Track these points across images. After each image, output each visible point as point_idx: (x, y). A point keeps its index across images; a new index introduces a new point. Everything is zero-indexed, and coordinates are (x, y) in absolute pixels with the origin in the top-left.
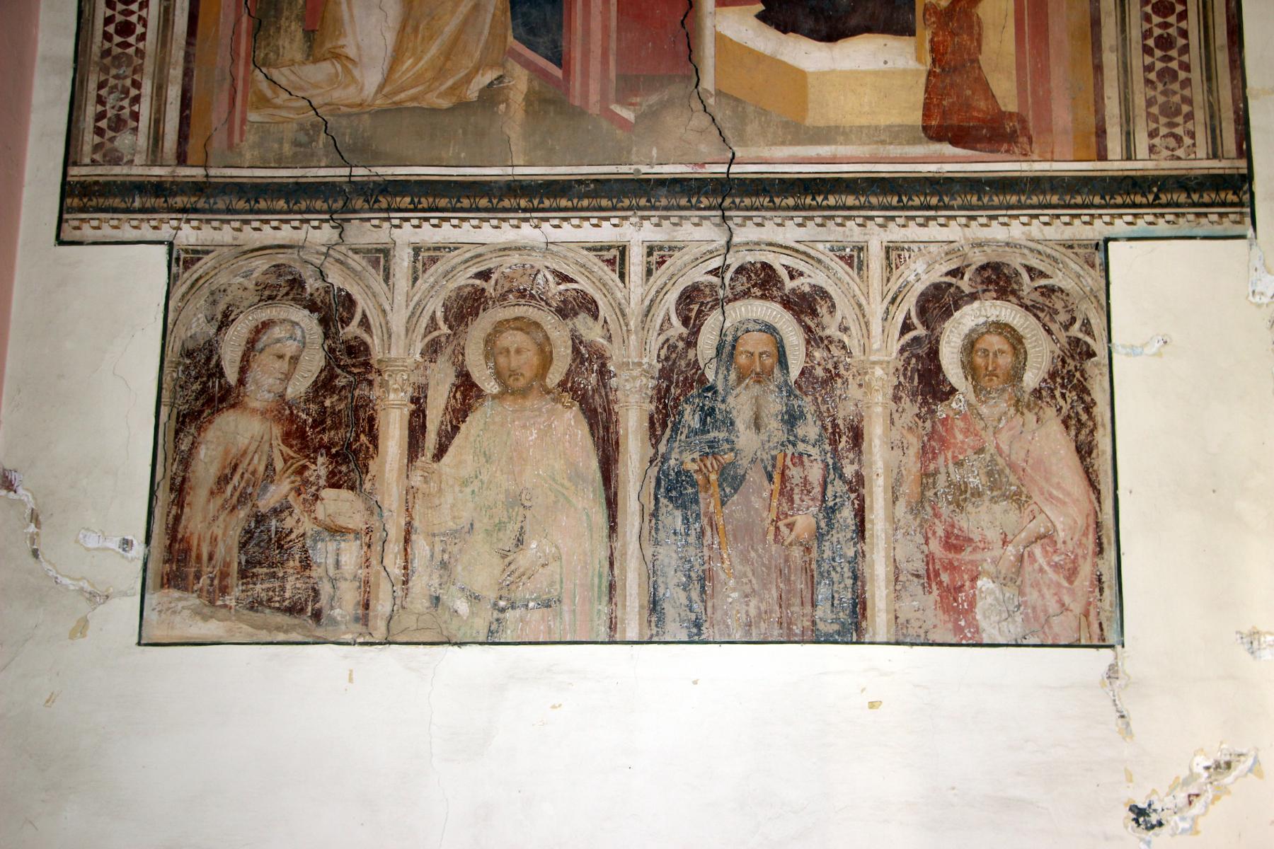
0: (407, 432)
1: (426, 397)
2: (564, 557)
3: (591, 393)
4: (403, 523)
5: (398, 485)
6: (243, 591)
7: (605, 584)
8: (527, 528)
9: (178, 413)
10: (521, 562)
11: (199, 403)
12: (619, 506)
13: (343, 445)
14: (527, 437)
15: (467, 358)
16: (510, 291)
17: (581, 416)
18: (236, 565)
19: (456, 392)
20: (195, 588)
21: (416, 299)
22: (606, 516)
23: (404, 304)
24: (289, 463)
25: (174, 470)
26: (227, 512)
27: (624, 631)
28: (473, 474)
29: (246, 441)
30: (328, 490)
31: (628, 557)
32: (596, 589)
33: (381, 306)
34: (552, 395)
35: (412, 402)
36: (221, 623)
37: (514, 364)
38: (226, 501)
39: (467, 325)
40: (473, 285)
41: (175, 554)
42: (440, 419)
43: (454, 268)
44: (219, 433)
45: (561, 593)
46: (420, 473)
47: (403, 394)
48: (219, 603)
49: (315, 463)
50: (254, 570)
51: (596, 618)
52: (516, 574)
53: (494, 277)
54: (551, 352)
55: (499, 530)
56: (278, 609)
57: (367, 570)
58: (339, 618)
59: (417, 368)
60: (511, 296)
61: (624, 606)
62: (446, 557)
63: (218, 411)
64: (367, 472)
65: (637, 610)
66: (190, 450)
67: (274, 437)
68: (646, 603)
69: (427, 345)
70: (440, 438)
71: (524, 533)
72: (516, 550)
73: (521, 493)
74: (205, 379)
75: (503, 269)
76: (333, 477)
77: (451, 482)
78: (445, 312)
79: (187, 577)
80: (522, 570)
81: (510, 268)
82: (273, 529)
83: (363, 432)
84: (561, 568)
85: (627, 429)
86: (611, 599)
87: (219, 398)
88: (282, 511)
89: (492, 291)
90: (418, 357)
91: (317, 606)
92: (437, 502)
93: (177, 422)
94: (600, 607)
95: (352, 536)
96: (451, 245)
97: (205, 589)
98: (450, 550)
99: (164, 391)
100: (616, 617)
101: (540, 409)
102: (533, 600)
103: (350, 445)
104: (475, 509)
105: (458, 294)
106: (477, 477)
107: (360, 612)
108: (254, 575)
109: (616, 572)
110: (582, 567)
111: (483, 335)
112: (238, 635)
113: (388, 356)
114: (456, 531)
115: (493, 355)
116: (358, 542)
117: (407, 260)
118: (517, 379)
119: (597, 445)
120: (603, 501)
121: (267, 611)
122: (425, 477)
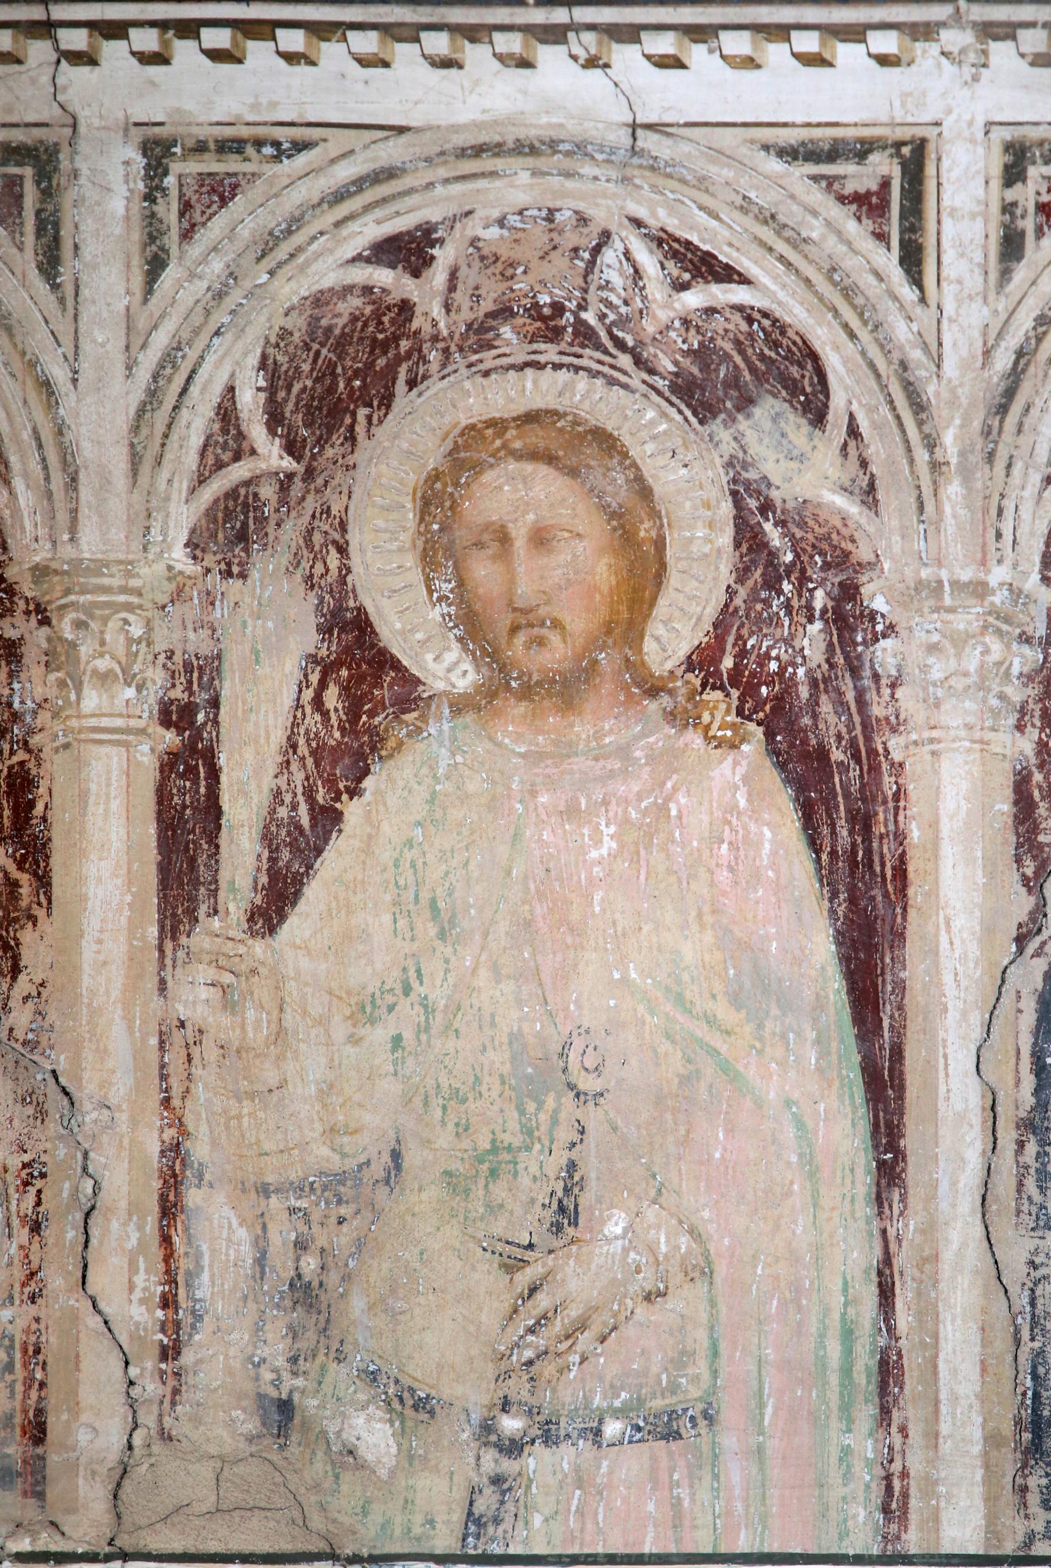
0: (152, 830)
1: (215, 703)
2: (721, 1270)
3: (804, 692)
4: (154, 1148)
7: (865, 1361)
8: (591, 1168)
10: (573, 1285)
12: (912, 1092)
14: (583, 851)
15: (356, 561)
16: (504, 312)
17: (772, 778)
19: (323, 685)
21: (161, 340)
22: (864, 1127)
23: (119, 360)
27: (935, 1518)
28: (393, 980)
31: (946, 1268)
32: (834, 1379)
33: (32, 364)
34: (665, 700)
35: (166, 721)
37: (525, 590)
39: (351, 438)
40: (368, 290)
42: (268, 782)
43: (294, 223)
45: (714, 1390)
46: (204, 973)
47: (130, 693)
51: (835, 1476)
52: (557, 1326)
53: (444, 256)
54: (660, 544)
55: (493, 1173)
59: (178, 595)
60: (506, 332)
61: (933, 1437)
62: (310, 1264)
65: (977, 1449)
68: (1007, 1428)
69: (210, 513)
70: (274, 852)
71: (581, 1184)
72: (557, 1243)
73: (567, 1045)
75: (474, 228)
77: (316, 1009)
78: (271, 390)
80: (574, 1312)
81: (501, 222)
84: (713, 1304)
85: (934, 825)
86: (885, 1412)
89: (437, 310)
90: (179, 556)
92: (272, 1077)
94: (848, 1440)
96: (280, 133)
98: (322, 1241)
100: (904, 1475)
101: (624, 752)
102: (618, 1413)
104: (407, 1101)
105: (314, 322)
106: (407, 990)
109: (903, 1320)
110: (783, 1304)
111: (413, 478)
113: (67, 551)
114: (341, 1178)
115: (449, 551)
117: (122, 190)
118: (541, 642)
119: (827, 878)
120: (855, 1076)
122: (224, 989)
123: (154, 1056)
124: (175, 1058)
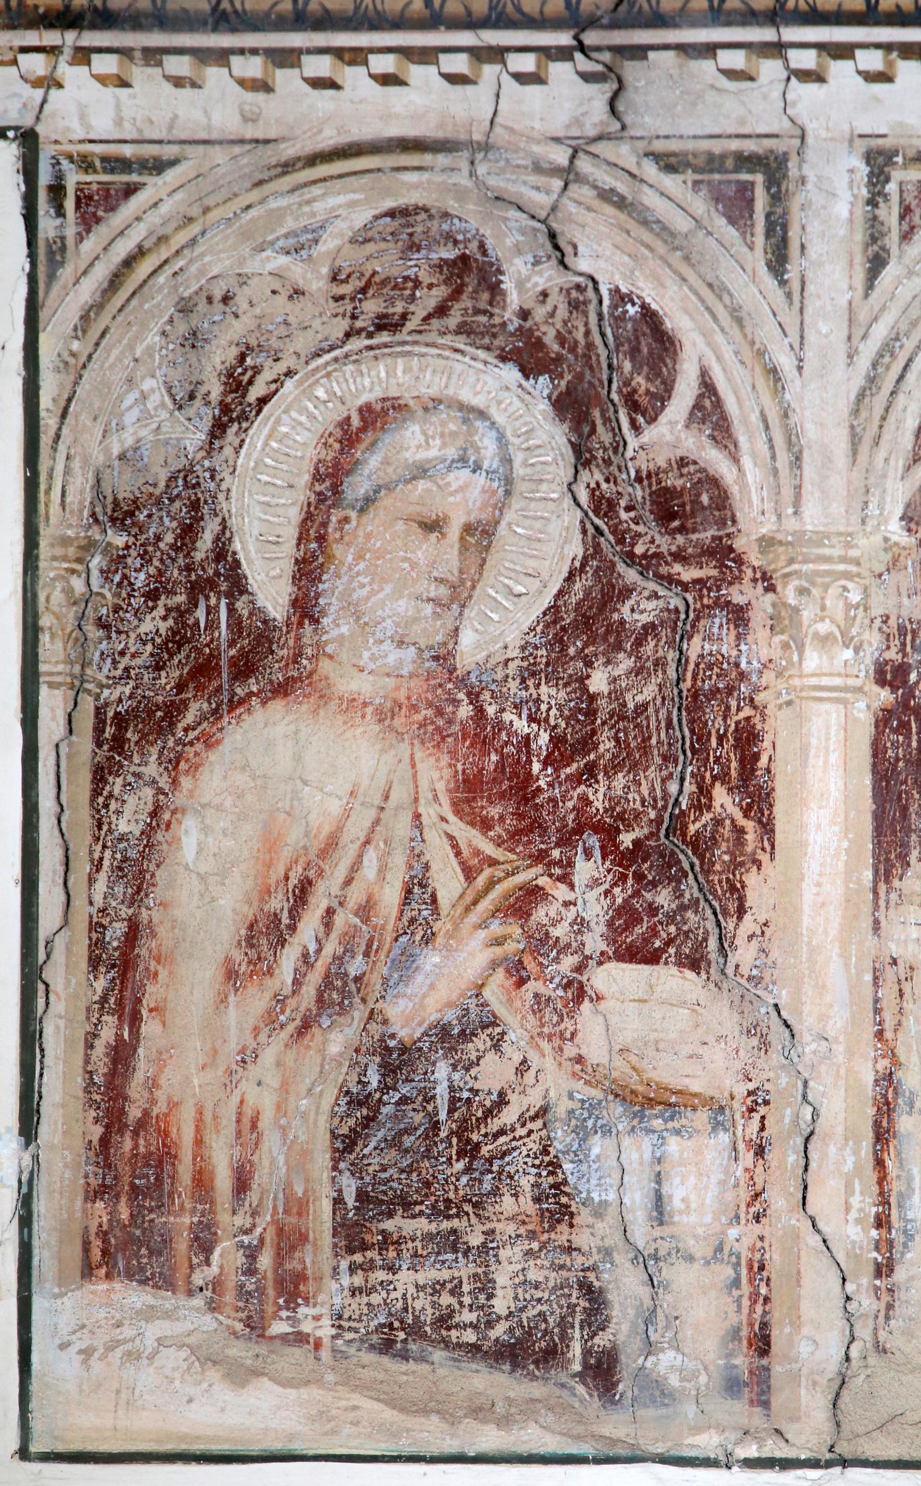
4: (870, 1078)
5: (845, 956)
6: (354, 1291)
9: (99, 712)
11: (169, 678)
13: (659, 821)
18: (326, 1207)
20: (198, 1279)
24: (481, 881)
25: (99, 900)
26: (284, 1035)
29: (335, 807)
30: (613, 967)
36: (292, 1393)
38: (280, 1000)
41: (125, 1170)
44: (240, 779)
48: (279, 1327)
49: (566, 879)
50: (389, 1225)
56: (474, 1349)
57: (757, 1229)
58: (674, 1381)
63: (234, 704)
64: (741, 911)
66: (149, 832)
67: (425, 795)
74: (181, 599)
76: (628, 927)
79: (167, 1241)
82: (442, 1092)
83: (723, 777)
87: (233, 661)
88: (466, 1036)
91: (601, 1341)
93: (99, 744)
95: (702, 1117)
97: (231, 1282)
99: (45, 638)
103: (678, 824)
107: (742, 1361)
108: (387, 1241)
112: (347, 1430)
116: (724, 1138)
121: (439, 1355)
123: (868, 991)
124: (888, 993)
